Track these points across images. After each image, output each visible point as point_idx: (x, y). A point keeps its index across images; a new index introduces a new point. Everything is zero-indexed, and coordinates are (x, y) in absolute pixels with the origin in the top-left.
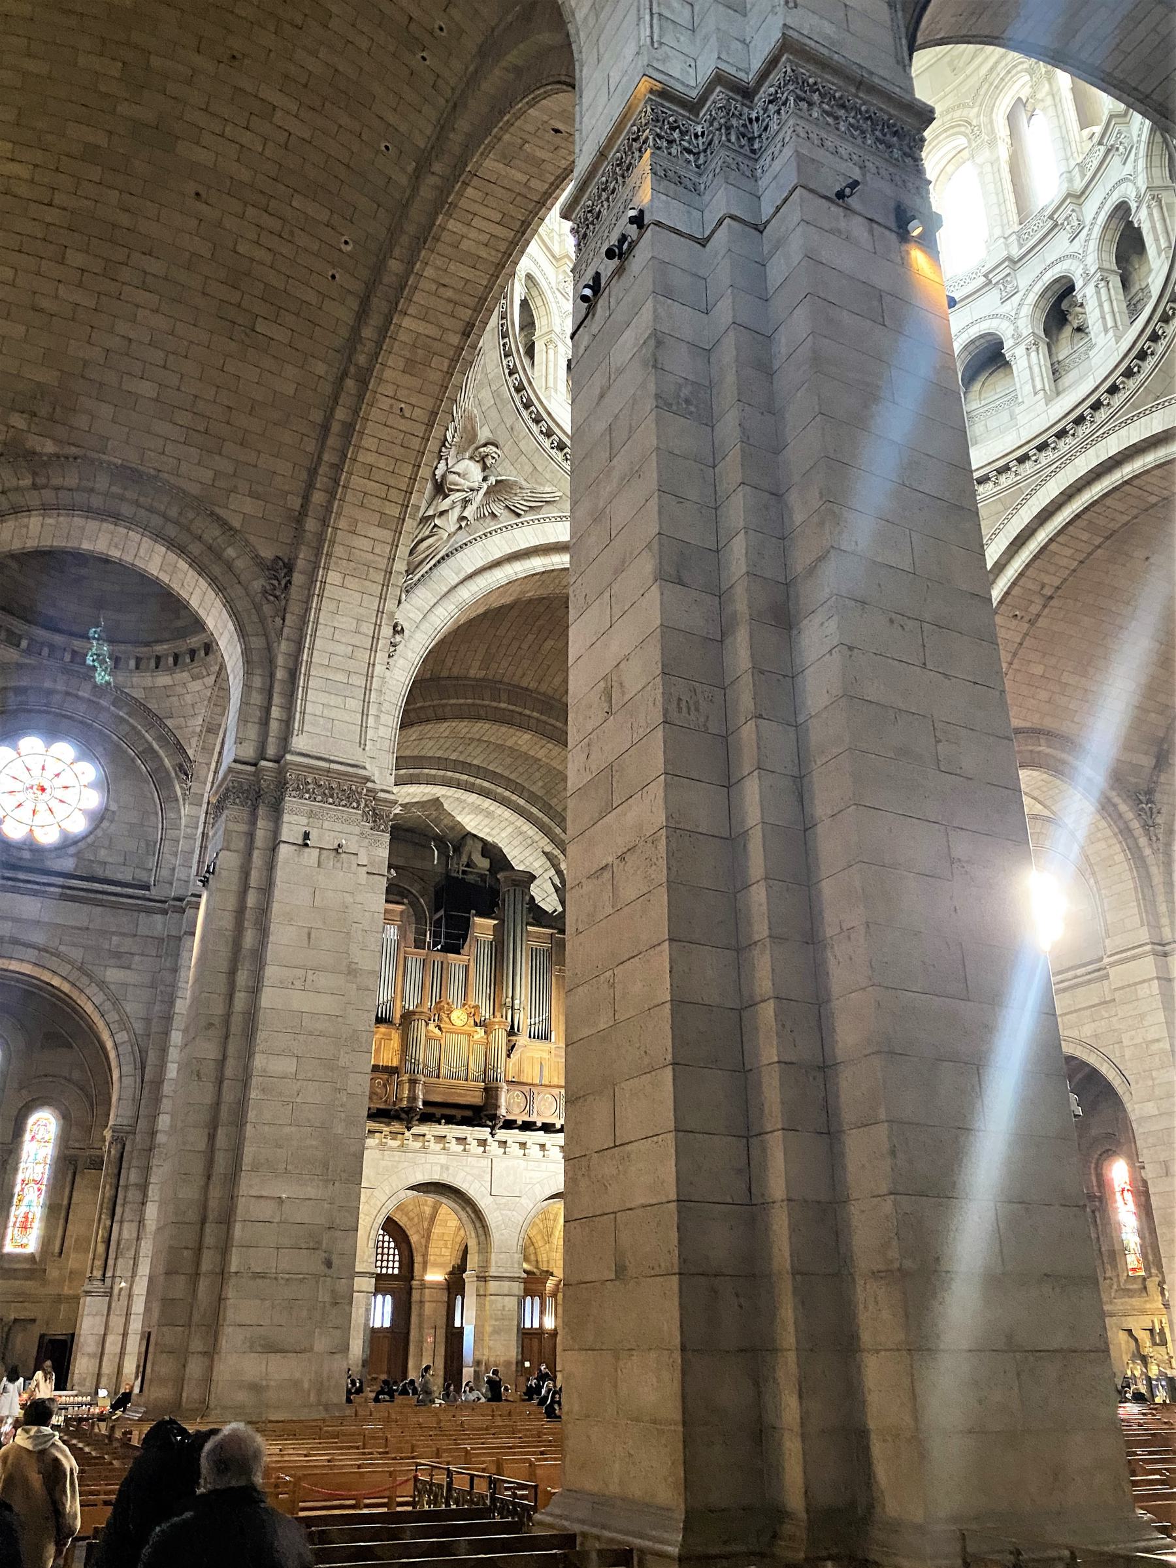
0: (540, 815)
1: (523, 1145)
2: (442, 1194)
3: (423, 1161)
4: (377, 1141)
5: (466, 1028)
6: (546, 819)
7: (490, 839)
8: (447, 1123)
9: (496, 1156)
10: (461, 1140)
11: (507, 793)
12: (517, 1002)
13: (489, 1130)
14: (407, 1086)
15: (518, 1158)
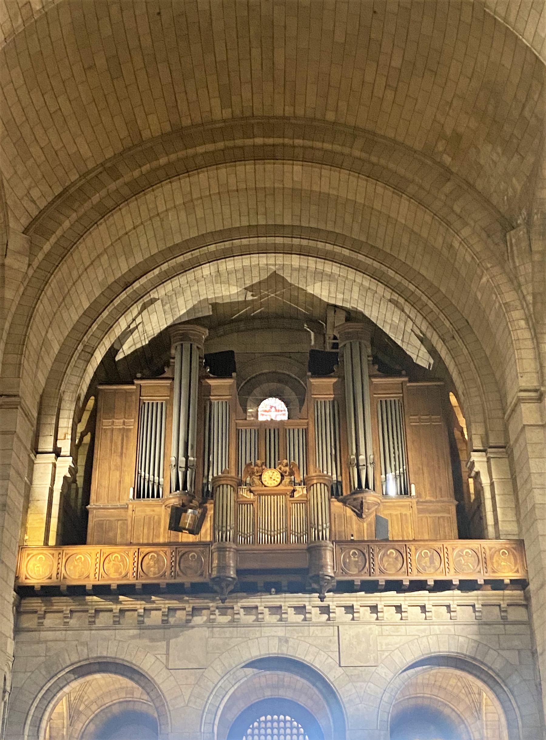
0: (369, 261)
1: (374, 609)
2: (287, 670)
3: (258, 635)
4: (205, 618)
5: (281, 487)
6: (376, 264)
7: (348, 305)
8: (277, 593)
9: (343, 623)
10: (301, 609)
11: (329, 247)
12: (362, 457)
13: (317, 595)
14: (215, 555)
15: (369, 623)
